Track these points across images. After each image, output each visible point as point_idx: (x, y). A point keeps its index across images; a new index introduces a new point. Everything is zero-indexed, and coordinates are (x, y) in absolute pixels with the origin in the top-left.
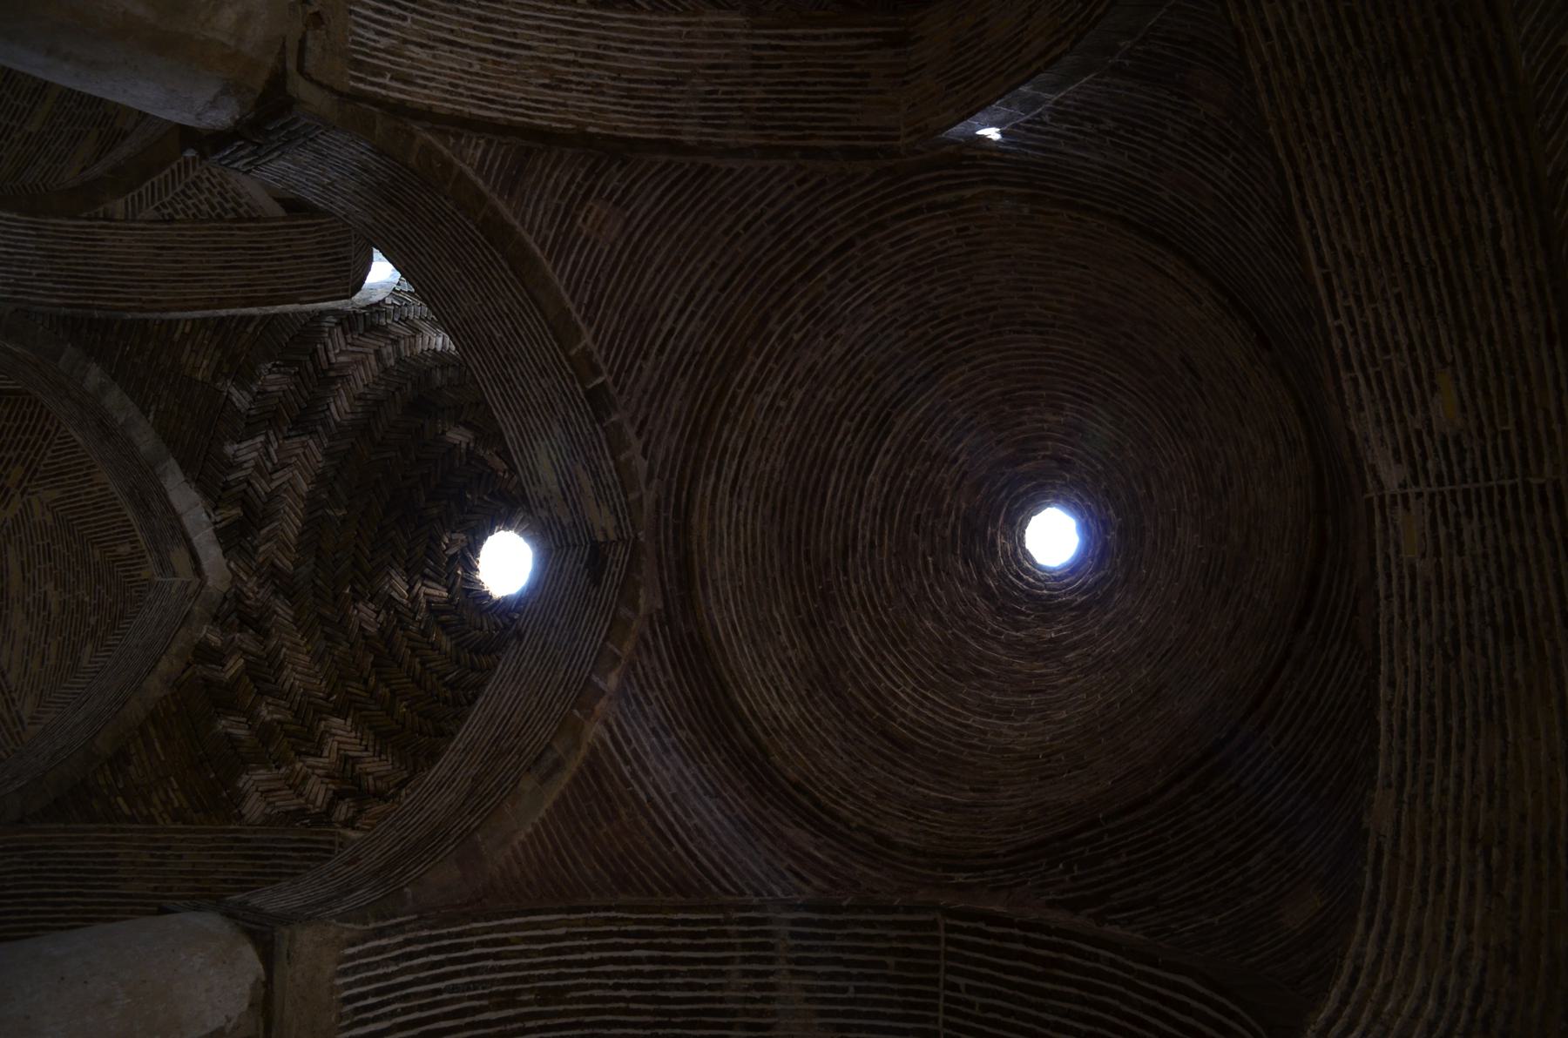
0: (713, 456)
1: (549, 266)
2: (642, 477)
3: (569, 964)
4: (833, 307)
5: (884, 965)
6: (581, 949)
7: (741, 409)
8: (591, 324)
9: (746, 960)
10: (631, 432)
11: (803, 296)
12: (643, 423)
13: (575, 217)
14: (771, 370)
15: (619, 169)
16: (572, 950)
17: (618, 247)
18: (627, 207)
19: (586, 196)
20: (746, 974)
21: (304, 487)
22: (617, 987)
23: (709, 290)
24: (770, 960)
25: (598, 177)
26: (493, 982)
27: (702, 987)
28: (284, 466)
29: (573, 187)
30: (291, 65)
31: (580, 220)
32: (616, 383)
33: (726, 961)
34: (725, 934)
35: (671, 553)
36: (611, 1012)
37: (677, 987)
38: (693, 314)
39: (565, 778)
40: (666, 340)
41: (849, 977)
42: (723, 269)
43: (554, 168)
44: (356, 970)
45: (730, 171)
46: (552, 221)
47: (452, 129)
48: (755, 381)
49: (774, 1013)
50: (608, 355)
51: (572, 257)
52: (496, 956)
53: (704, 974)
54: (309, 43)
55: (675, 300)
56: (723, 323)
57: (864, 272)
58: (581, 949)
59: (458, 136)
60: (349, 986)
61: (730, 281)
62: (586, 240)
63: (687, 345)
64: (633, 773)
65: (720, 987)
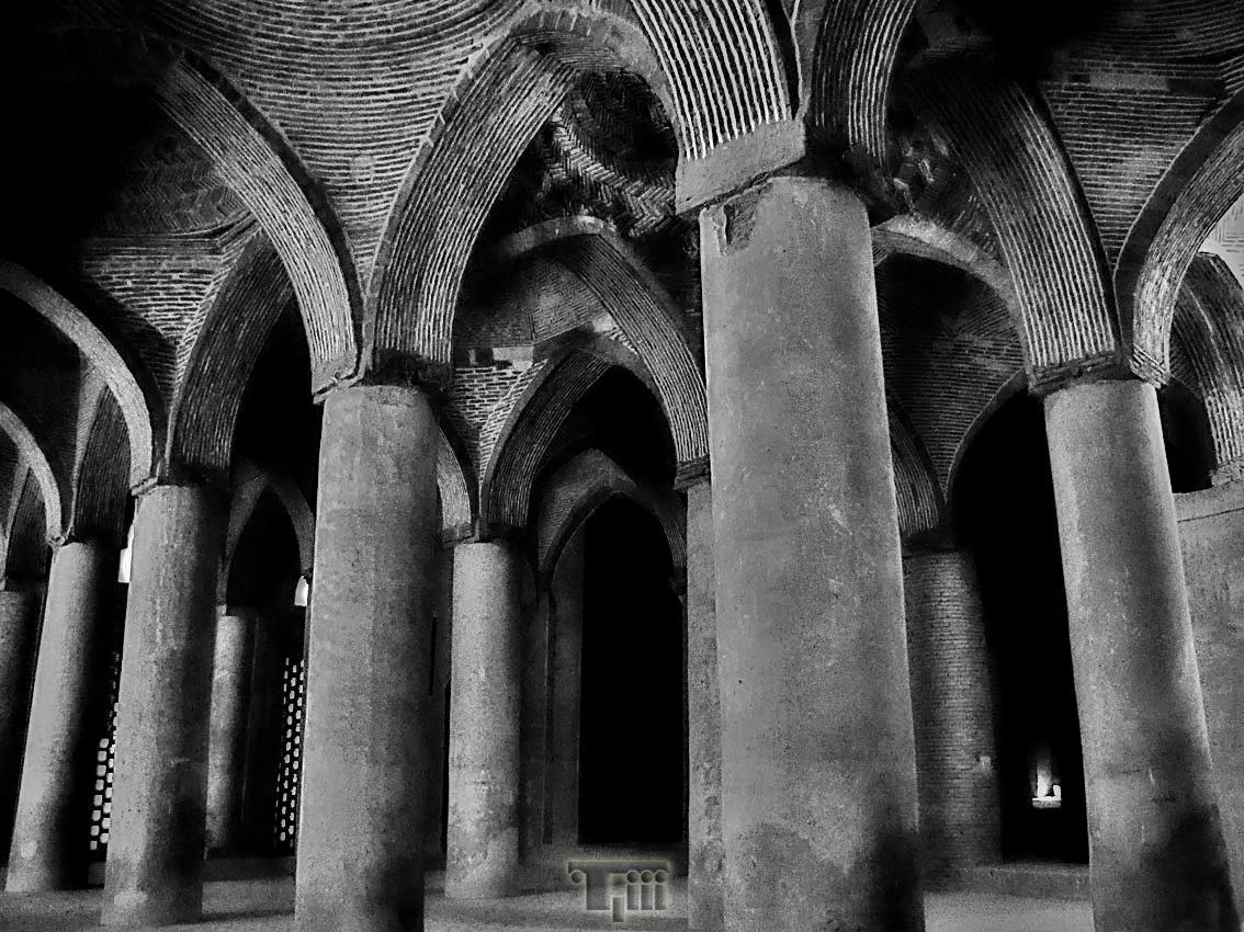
0: (438, 19)
1: (400, 185)
2: (478, 53)
4: (305, 12)
7: (402, 20)
8: (418, 141)
10: (459, 77)
11: (312, 36)
12: (449, 73)
13: (369, 186)
14: (368, 19)
15: (328, 180)
17: (370, 151)
18: (347, 162)
19: (354, 187)
23: (354, 87)
25: (340, 188)
26: (693, 34)
29: (355, 197)
30: (354, 380)
31: (369, 182)
32: (439, 105)
35: (505, 7)
38: (374, 86)
40: (397, 91)
42: (336, 88)
43: (351, 214)
45: (282, 125)
46: (377, 198)
47: (359, 280)
48: (379, 24)
50: (428, 119)
51: (391, 174)
55: (375, 101)
56: (365, 66)
57: (267, 13)
59: (362, 275)
60: (708, 144)
61: (339, 80)
62: (377, 172)
63: (392, 77)
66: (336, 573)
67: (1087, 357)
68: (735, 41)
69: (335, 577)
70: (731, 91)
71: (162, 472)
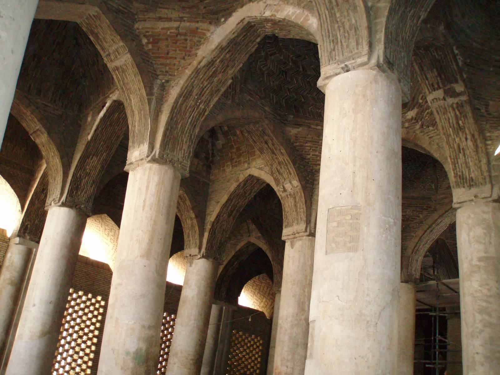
30: (490, 199)
54: (483, 196)
66: (487, 284)
69: (487, 287)
71: (310, 230)
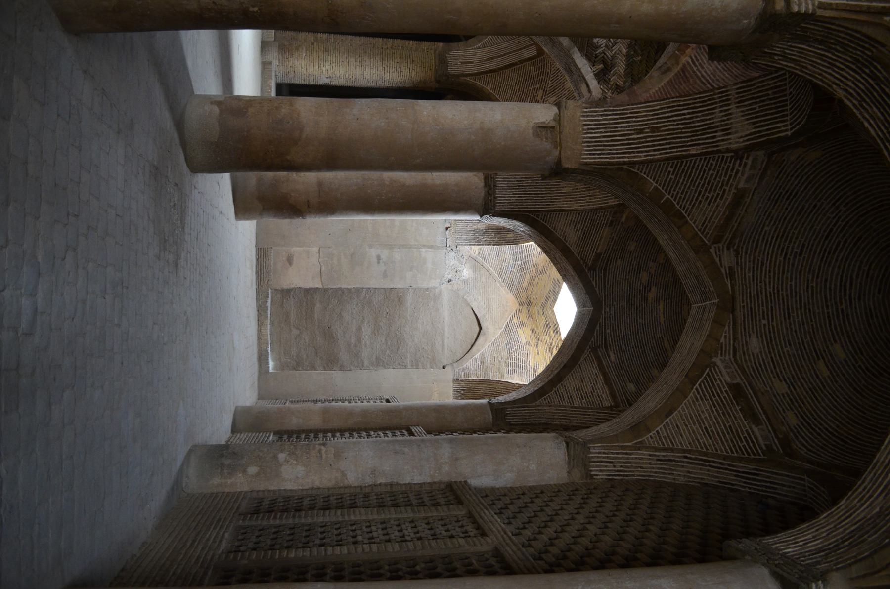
3: (661, 118)
5: (768, 95)
6: (664, 113)
9: (721, 107)
16: (662, 113)
20: (721, 111)
21: (624, 51)
22: (678, 125)
24: (729, 105)
27: (706, 120)
28: (616, 43)
33: (714, 109)
34: (714, 99)
36: (676, 134)
37: (698, 121)
39: (671, 75)
41: (756, 103)
44: (588, 116)
49: (731, 123)
52: (636, 117)
53: (707, 115)
58: (664, 113)
64: (698, 69)
65: (712, 118)
67: (495, 198)
68: (623, 145)
70: (604, 137)
